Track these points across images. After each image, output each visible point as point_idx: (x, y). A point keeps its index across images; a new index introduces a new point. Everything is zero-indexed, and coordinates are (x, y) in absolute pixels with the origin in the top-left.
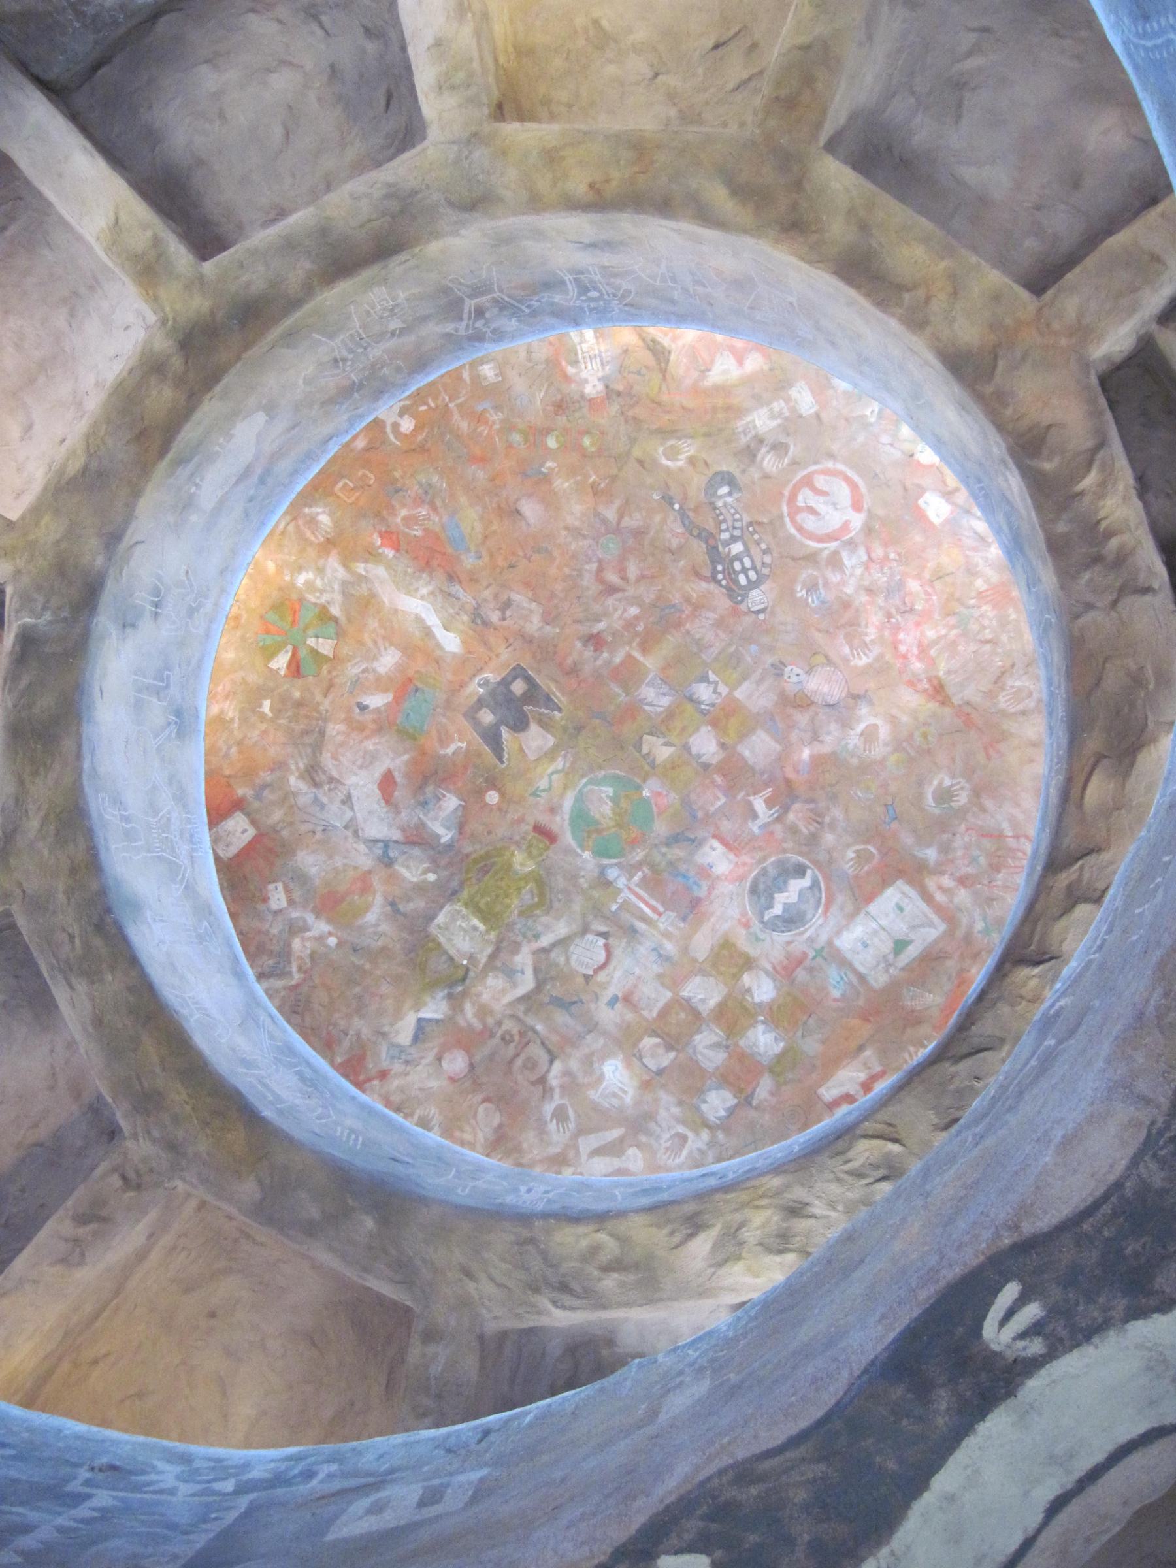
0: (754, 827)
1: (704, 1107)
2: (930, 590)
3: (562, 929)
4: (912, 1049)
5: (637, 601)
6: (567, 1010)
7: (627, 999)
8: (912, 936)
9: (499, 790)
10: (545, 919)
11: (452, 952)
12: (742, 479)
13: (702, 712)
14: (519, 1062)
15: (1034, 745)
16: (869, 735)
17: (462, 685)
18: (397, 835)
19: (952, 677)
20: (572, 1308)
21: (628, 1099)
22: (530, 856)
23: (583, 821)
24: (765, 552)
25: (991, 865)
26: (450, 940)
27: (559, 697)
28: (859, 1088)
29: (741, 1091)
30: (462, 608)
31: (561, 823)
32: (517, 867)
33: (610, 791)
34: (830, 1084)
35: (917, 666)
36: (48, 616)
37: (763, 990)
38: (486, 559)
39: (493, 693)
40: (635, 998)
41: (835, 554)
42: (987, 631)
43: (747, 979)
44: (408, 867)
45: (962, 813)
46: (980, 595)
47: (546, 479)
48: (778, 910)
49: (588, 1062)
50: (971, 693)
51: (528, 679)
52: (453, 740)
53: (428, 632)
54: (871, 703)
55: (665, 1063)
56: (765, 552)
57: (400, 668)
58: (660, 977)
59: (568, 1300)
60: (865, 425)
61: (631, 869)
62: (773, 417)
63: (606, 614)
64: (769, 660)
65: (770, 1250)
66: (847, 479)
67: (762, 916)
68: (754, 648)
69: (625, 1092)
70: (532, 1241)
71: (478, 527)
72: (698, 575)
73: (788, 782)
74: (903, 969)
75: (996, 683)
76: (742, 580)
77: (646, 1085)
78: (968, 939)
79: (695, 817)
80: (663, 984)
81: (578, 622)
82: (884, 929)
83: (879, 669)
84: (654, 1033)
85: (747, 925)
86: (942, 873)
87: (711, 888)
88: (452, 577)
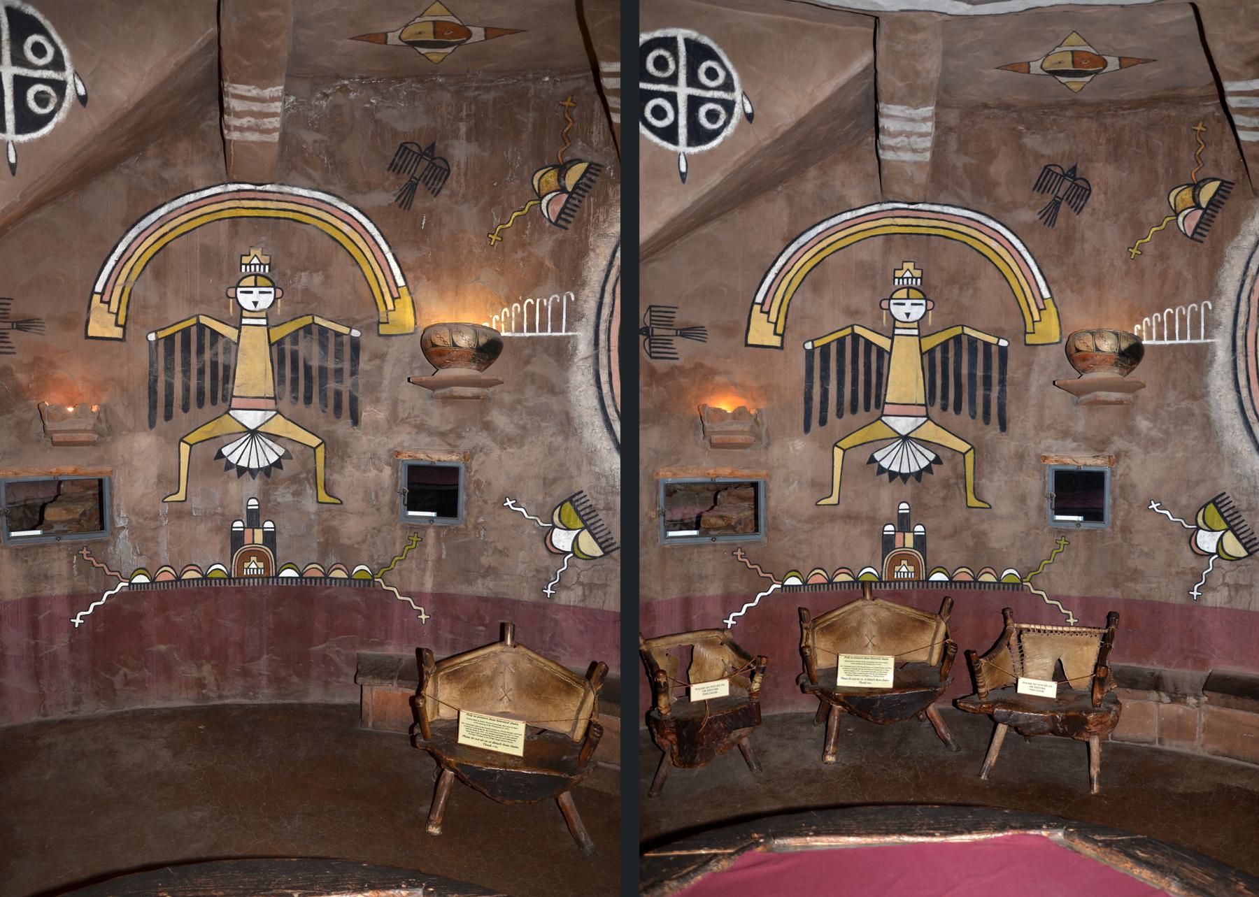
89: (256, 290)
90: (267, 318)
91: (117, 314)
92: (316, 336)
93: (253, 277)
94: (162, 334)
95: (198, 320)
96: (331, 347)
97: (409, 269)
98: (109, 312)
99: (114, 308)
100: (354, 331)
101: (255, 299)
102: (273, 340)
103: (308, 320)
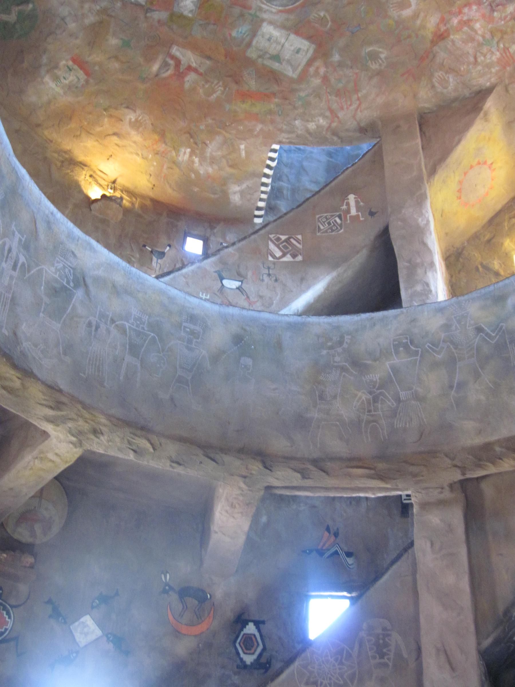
2: (508, 18)
4: (221, 83)
8: (284, 63)
15: (415, 96)
19: (450, 43)
25: (339, 90)
28: (186, 65)
34: (181, 49)
35: (455, 21)
42: (482, 58)
50: (442, 56)
74: (263, 65)
75: (450, 69)
78: (293, 91)
82: (283, 46)
86: (327, 67)
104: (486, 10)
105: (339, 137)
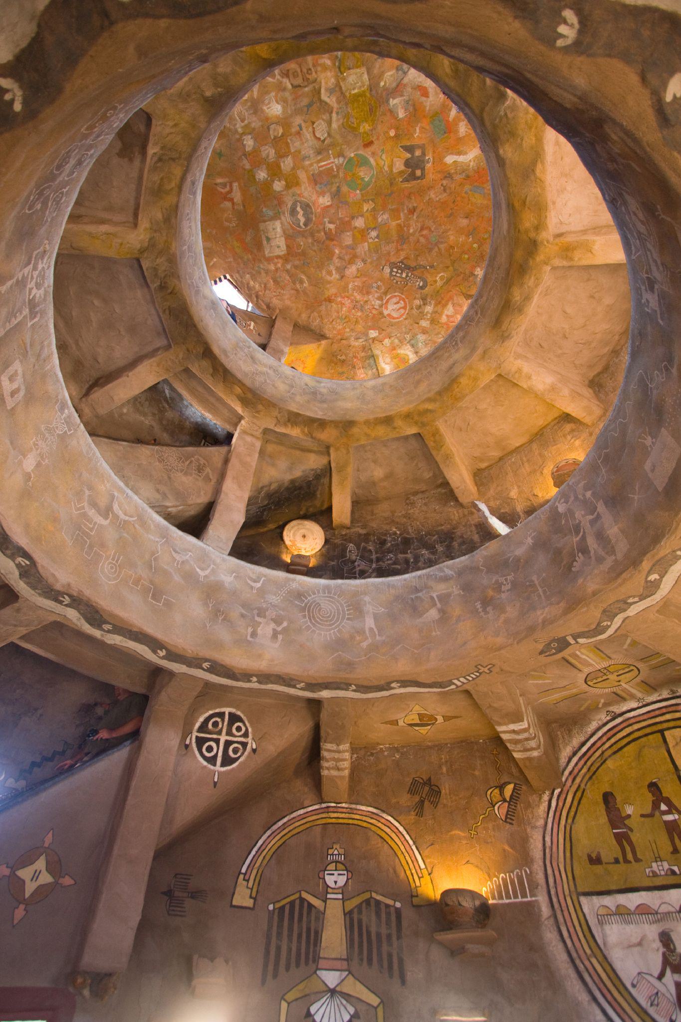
0: (326, 220)
1: (250, 137)
3: (335, 125)
5: (413, 234)
6: (307, 106)
7: (298, 133)
9: (393, 137)
10: (341, 121)
11: (352, 71)
12: (420, 291)
13: (369, 228)
14: (299, 71)
16: (330, 273)
17: (434, 152)
18: (405, 81)
20: (152, 159)
21: (265, 108)
22: (365, 133)
23: (363, 162)
24: (397, 282)
26: (356, 74)
27: (406, 185)
29: (249, 155)
30: (456, 173)
31: (366, 153)
32: (365, 124)
33: (366, 180)
35: (339, 299)
36: (502, 113)
37: (278, 186)
38: (463, 195)
39: (423, 162)
40: (297, 137)
41: (382, 300)
43: (284, 183)
44: (391, 76)
45: (294, 283)
46: (345, 328)
47: (467, 236)
48: (298, 209)
49: (285, 101)
50: (323, 308)
51: (418, 178)
52: (421, 132)
53: (459, 153)
54: (338, 280)
55: (271, 132)
56: (397, 282)
57: (457, 131)
58: (300, 152)
59: (155, 159)
60: (405, 333)
61: (338, 168)
62: (428, 312)
63: (417, 221)
64: (369, 260)
65: (150, 239)
66: (397, 318)
67: (300, 203)
68: (375, 258)
69: (268, 108)
70: (179, 158)
71: (474, 200)
72: (406, 258)
73: (332, 240)
76: (395, 270)
77: (267, 119)
78: (260, 261)
79: (341, 202)
80: (296, 151)
81: (422, 210)
83: (345, 288)
84: (282, 135)
85: (299, 195)
87: (317, 192)
88: (468, 177)
89: (336, 873)
90: (342, 893)
91: (252, 889)
92: (373, 908)
93: (334, 864)
94: (278, 905)
95: (300, 894)
96: (383, 916)
97: (427, 856)
98: (247, 887)
99: (250, 884)
100: (397, 903)
101: (335, 879)
102: (346, 911)
103: (366, 896)
104: (352, 306)
105: (257, 301)
